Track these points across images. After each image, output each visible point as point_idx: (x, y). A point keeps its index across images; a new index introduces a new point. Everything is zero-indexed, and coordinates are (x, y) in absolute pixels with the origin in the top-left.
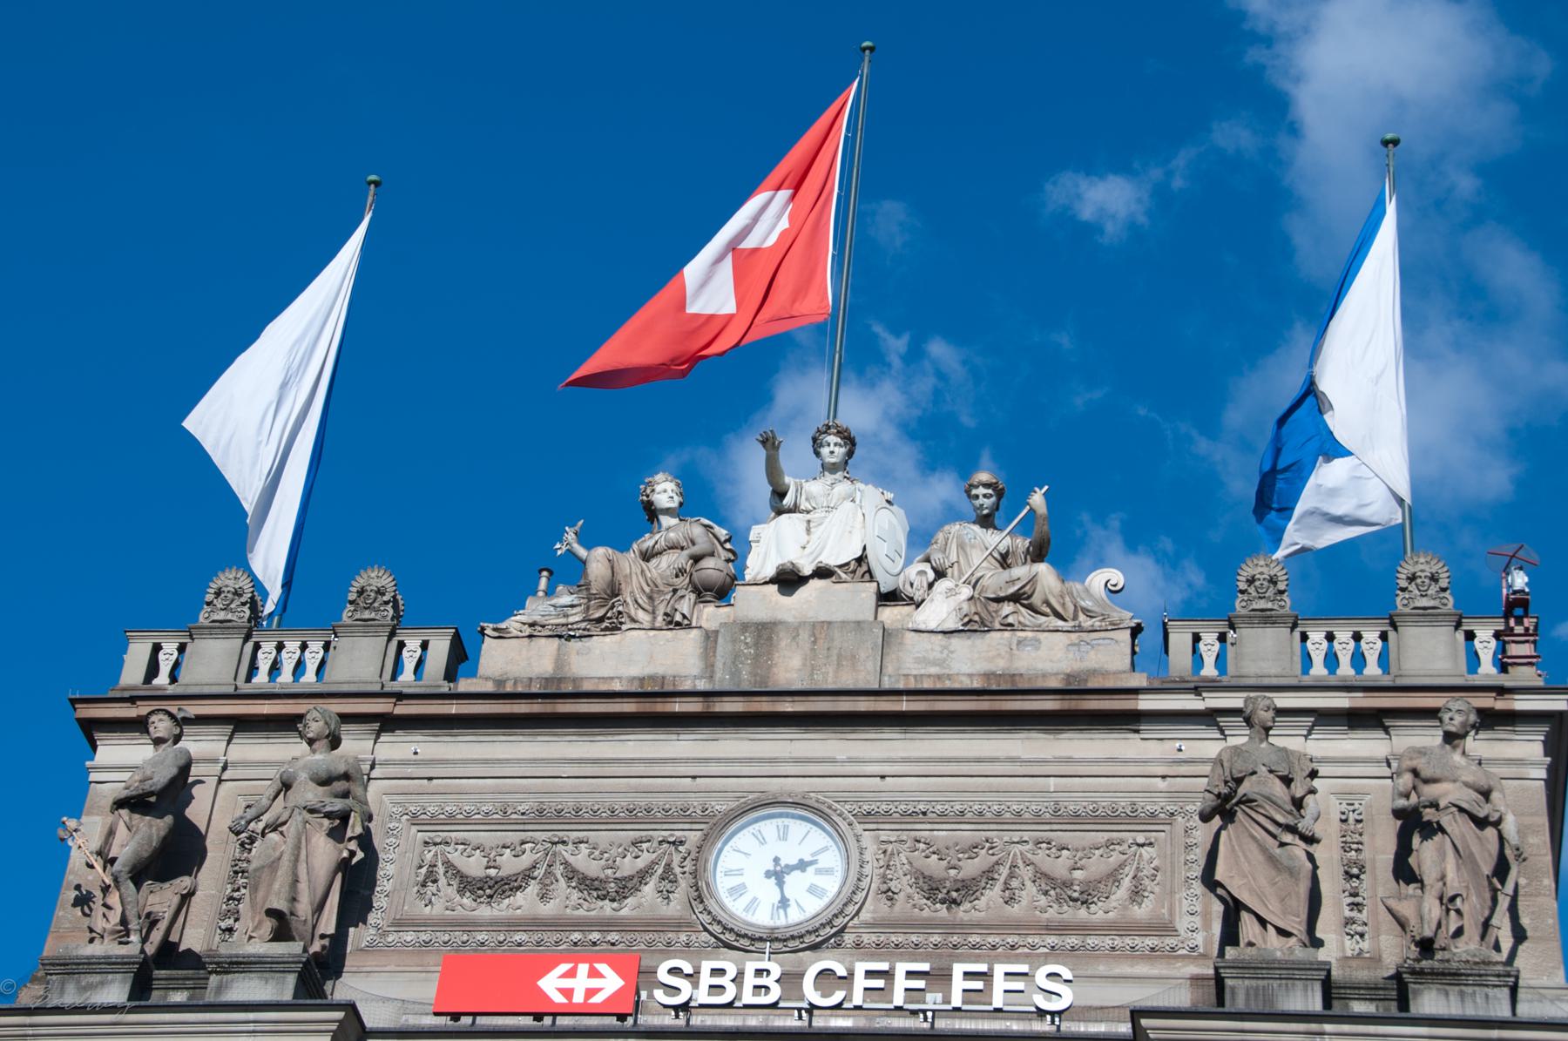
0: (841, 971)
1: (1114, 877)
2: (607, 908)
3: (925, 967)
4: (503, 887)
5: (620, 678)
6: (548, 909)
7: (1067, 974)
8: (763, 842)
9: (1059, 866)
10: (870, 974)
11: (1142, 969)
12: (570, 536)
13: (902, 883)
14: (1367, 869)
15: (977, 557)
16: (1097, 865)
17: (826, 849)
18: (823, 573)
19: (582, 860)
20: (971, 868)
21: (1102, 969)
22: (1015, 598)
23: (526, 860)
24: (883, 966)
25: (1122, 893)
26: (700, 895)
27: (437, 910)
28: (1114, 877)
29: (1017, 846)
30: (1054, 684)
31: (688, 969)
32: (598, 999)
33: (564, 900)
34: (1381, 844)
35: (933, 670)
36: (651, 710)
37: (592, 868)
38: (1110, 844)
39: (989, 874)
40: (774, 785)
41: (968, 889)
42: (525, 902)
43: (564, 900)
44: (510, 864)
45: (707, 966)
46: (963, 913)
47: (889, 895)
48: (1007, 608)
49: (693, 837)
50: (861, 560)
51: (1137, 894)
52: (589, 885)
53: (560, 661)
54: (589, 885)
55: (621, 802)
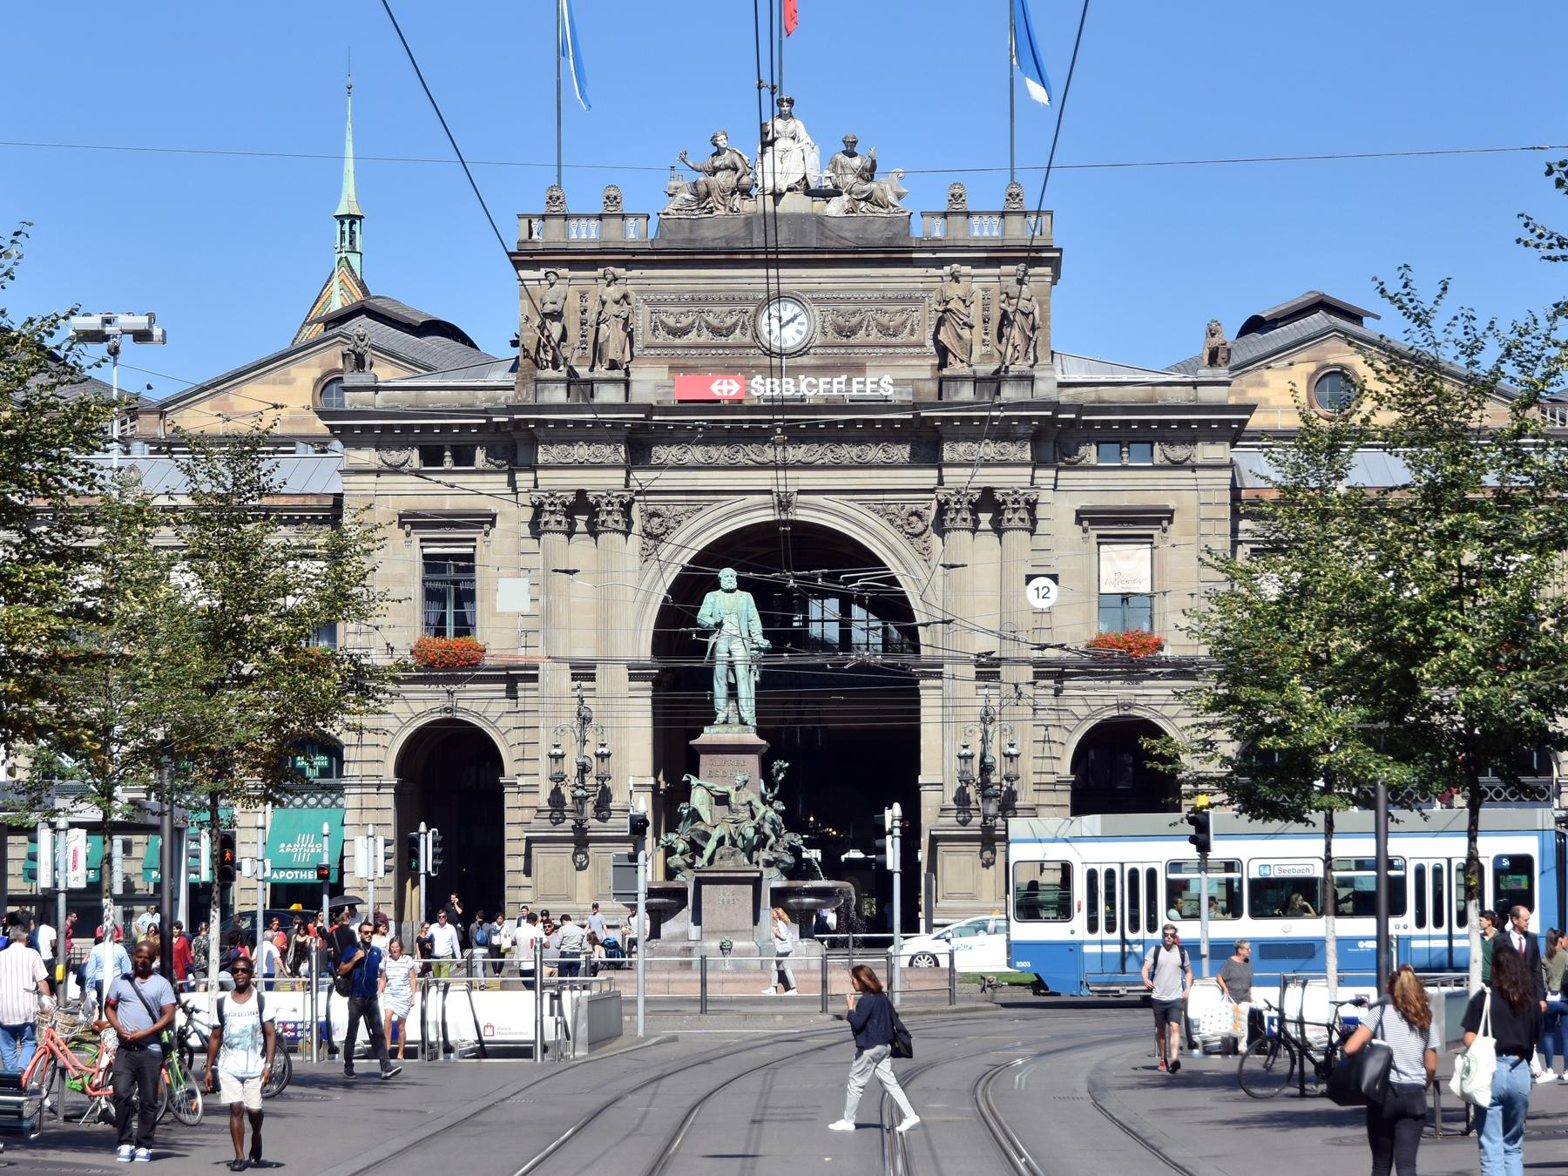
0: (814, 381)
1: (904, 324)
4: (685, 331)
6: (702, 340)
9: (885, 320)
11: (914, 362)
13: (829, 329)
15: (850, 178)
16: (898, 319)
18: (789, 190)
19: (710, 318)
20: (854, 321)
21: (901, 362)
22: (865, 200)
23: (690, 319)
25: (907, 331)
26: (756, 336)
27: (660, 341)
28: (904, 324)
29: (870, 312)
30: (881, 243)
33: (706, 338)
34: (996, 316)
37: (715, 322)
38: (902, 311)
39: (860, 325)
41: (854, 331)
42: (692, 337)
43: (706, 338)
44: (685, 321)
46: (852, 341)
47: (825, 334)
48: (862, 204)
49: (752, 309)
50: (804, 178)
51: (912, 332)
52: (716, 331)
54: (716, 331)
55: (722, 295)
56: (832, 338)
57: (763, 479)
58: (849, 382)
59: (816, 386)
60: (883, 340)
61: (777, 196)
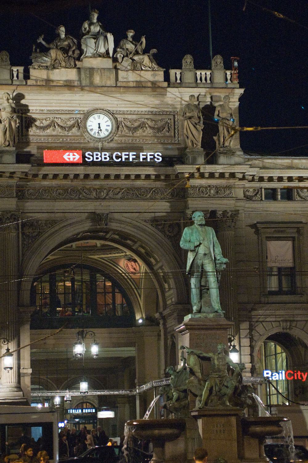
0: (120, 154)
2: (66, 133)
3: (135, 153)
5: (62, 81)
6: (54, 133)
7: (160, 155)
8: (95, 119)
10: (125, 155)
12: (41, 39)
14: (192, 94)
17: (108, 121)
19: (59, 122)
20: (136, 124)
24: (127, 153)
31: (91, 154)
32: (67, 154)
35: (125, 80)
37: (61, 124)
39: (139, 126)
40: (97, 106)
41: (135, 129)
45: (95, 153)
46: (135, 134)
53: (48, 76)
58: (138, 157)
59: (121, 157)
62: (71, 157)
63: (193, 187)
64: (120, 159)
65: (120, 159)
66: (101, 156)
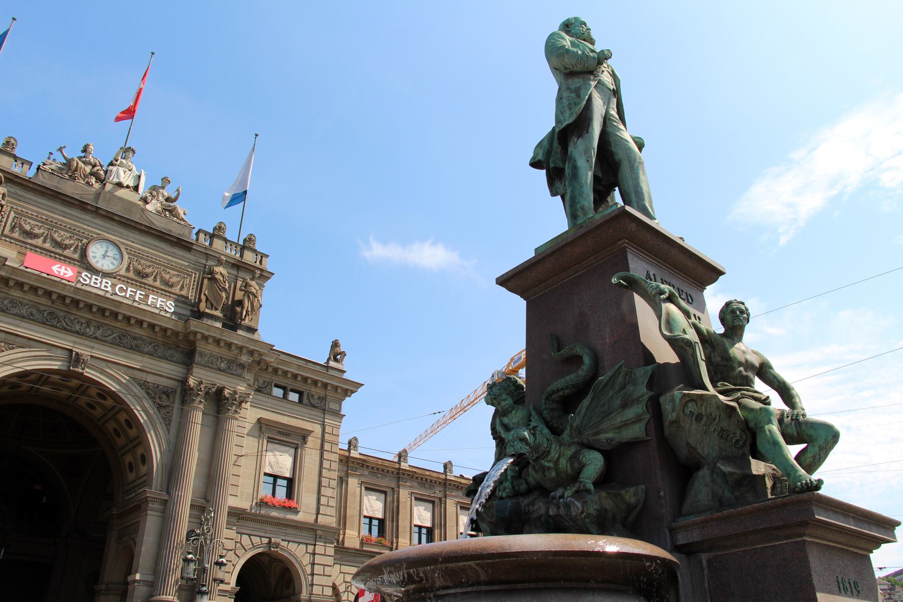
4: (36, 236)
6: (47, 245)
9: (167, 277)
18: (128, 187)
19: (56, 236)
22: (169, 211)
23: (42, 231)
25: (179, 287)
36: (82, 206)
41: (147, 276)
42: (39, 242)
44: (36, 231)
46: (144, 281)
56: (131, 275)
57: (65, 341)
59: (126, 291)
60: (163, 287)
61: (120, 185)
62: (63, 271)
63: (202, 355)
64: (123, 294)
65: (123, 294)
66: (101, 283)
